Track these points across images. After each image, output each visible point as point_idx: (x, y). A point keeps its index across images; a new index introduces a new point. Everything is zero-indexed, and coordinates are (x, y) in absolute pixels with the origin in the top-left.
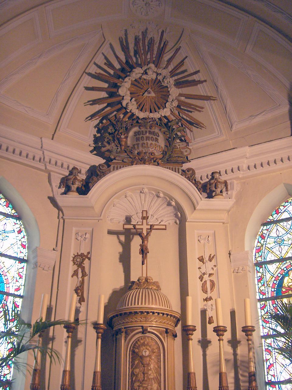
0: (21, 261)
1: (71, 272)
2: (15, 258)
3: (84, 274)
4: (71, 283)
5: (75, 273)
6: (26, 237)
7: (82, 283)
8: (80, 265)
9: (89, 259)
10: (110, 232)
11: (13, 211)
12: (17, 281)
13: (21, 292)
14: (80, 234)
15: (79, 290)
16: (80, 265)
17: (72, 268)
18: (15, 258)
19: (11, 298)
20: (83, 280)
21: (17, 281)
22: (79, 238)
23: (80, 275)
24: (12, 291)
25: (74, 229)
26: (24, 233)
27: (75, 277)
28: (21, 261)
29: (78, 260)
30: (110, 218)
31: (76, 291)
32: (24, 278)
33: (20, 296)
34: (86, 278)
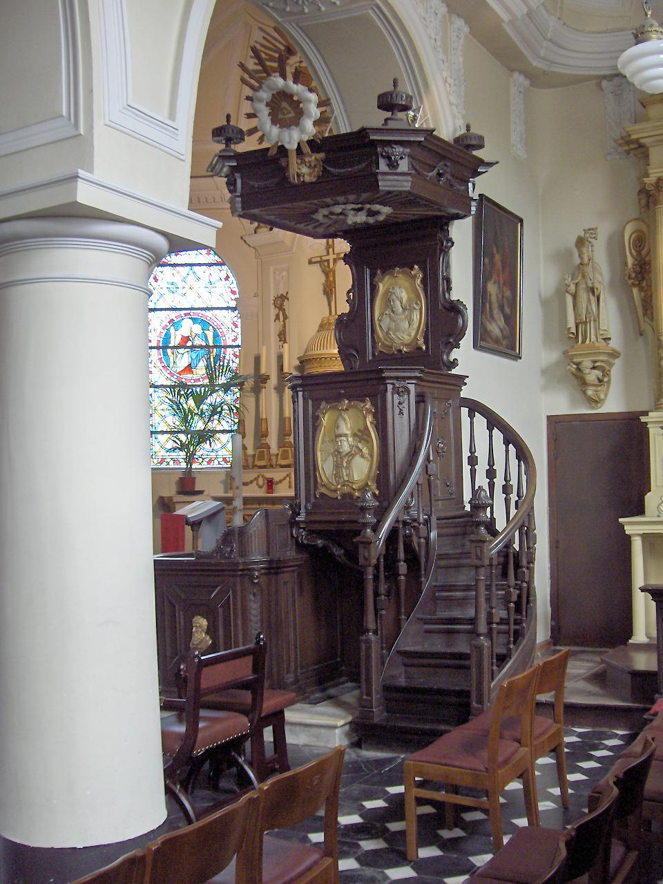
0: (234, 309)
1: (273, 317)
2: (227, 308)
3: (285, 317)
4: (274, 328)
5: (277, 317)
6: (235, 282)
7: (284, 326)
8: (281, 308)
9: (288, 299)
10: (310, 262)
11: (216, 258)
12: (233, 331)
13: (239, 342)
14: (277, 273)
15: (282, 336)
16: (281, 308)
17: (273, 312)
18: (227, 308)
19: (229, 350)
20: (285, 323)
21: (233, 331)
22: (277, 278)
23: (281, 318)
24: (229, 343)
25: (272, 269)
26: (232, 278)
27: (277, 321)
28: (234, 309)
29: (279, 302)
30: (308, 246)
31: (279, 335)
32: (239, 326)
33: (238, 346)
34: (287, 321)
